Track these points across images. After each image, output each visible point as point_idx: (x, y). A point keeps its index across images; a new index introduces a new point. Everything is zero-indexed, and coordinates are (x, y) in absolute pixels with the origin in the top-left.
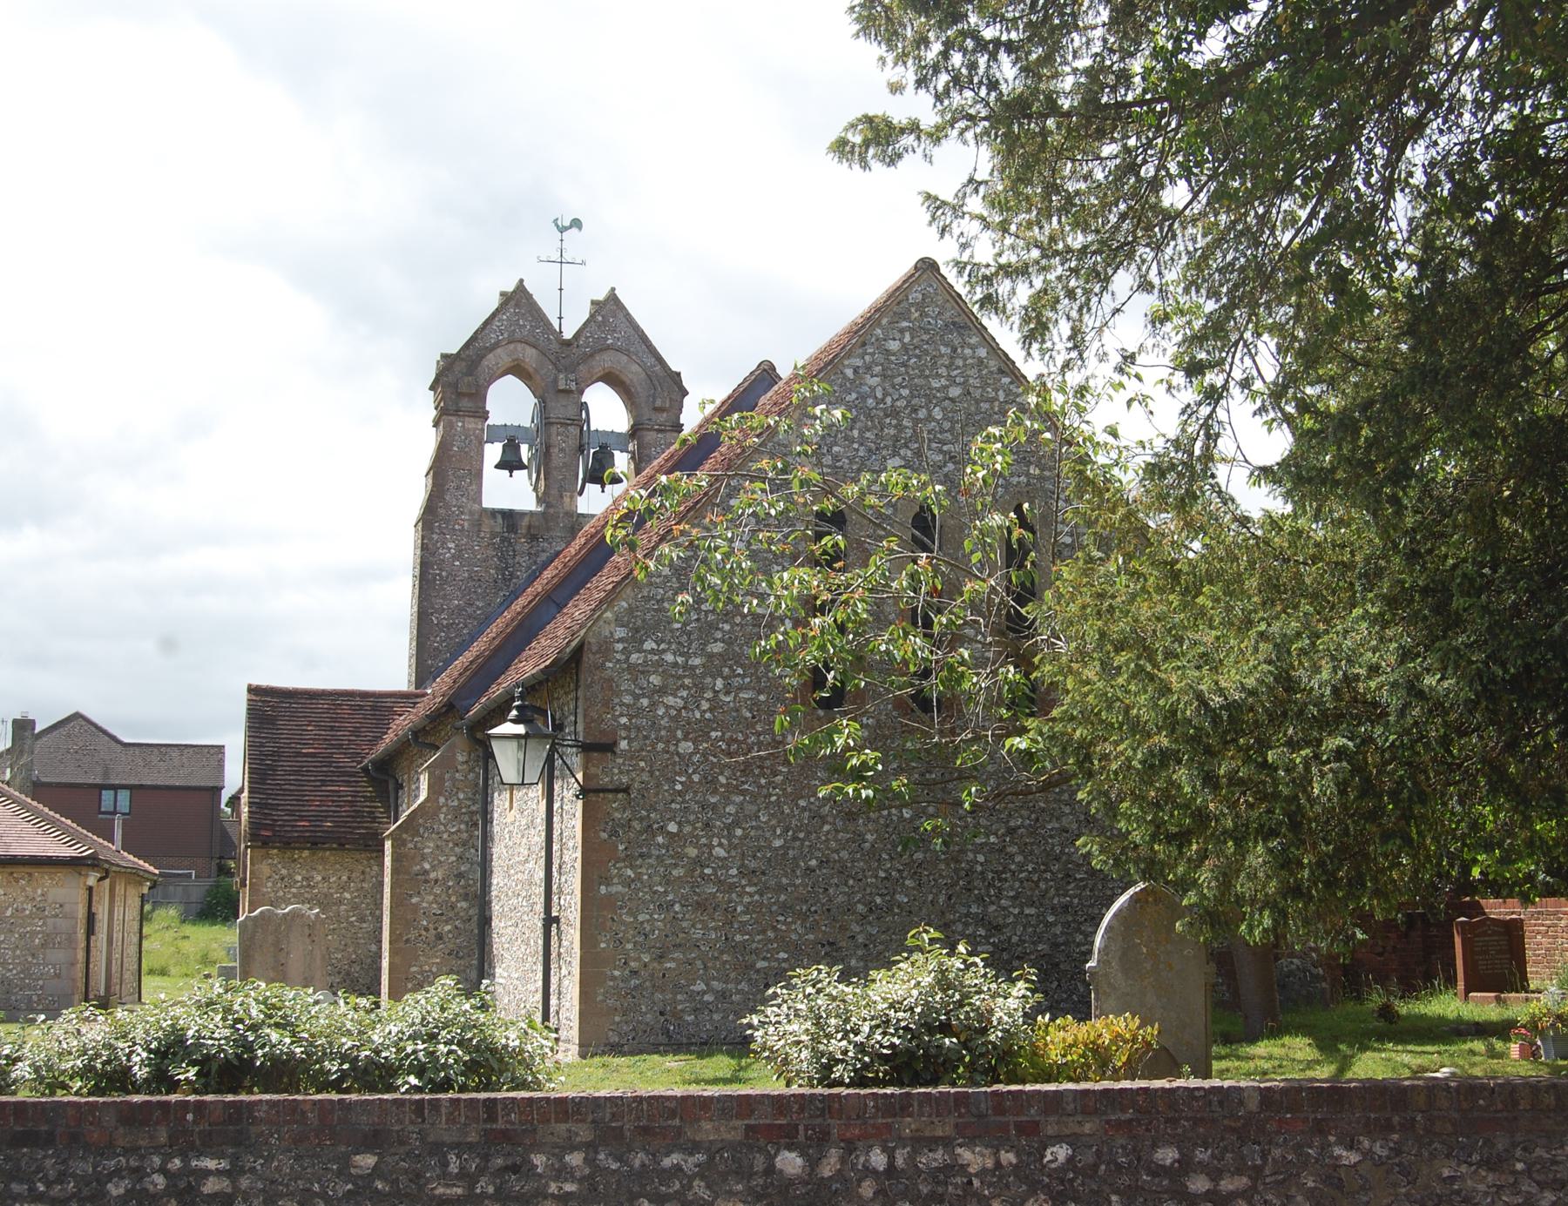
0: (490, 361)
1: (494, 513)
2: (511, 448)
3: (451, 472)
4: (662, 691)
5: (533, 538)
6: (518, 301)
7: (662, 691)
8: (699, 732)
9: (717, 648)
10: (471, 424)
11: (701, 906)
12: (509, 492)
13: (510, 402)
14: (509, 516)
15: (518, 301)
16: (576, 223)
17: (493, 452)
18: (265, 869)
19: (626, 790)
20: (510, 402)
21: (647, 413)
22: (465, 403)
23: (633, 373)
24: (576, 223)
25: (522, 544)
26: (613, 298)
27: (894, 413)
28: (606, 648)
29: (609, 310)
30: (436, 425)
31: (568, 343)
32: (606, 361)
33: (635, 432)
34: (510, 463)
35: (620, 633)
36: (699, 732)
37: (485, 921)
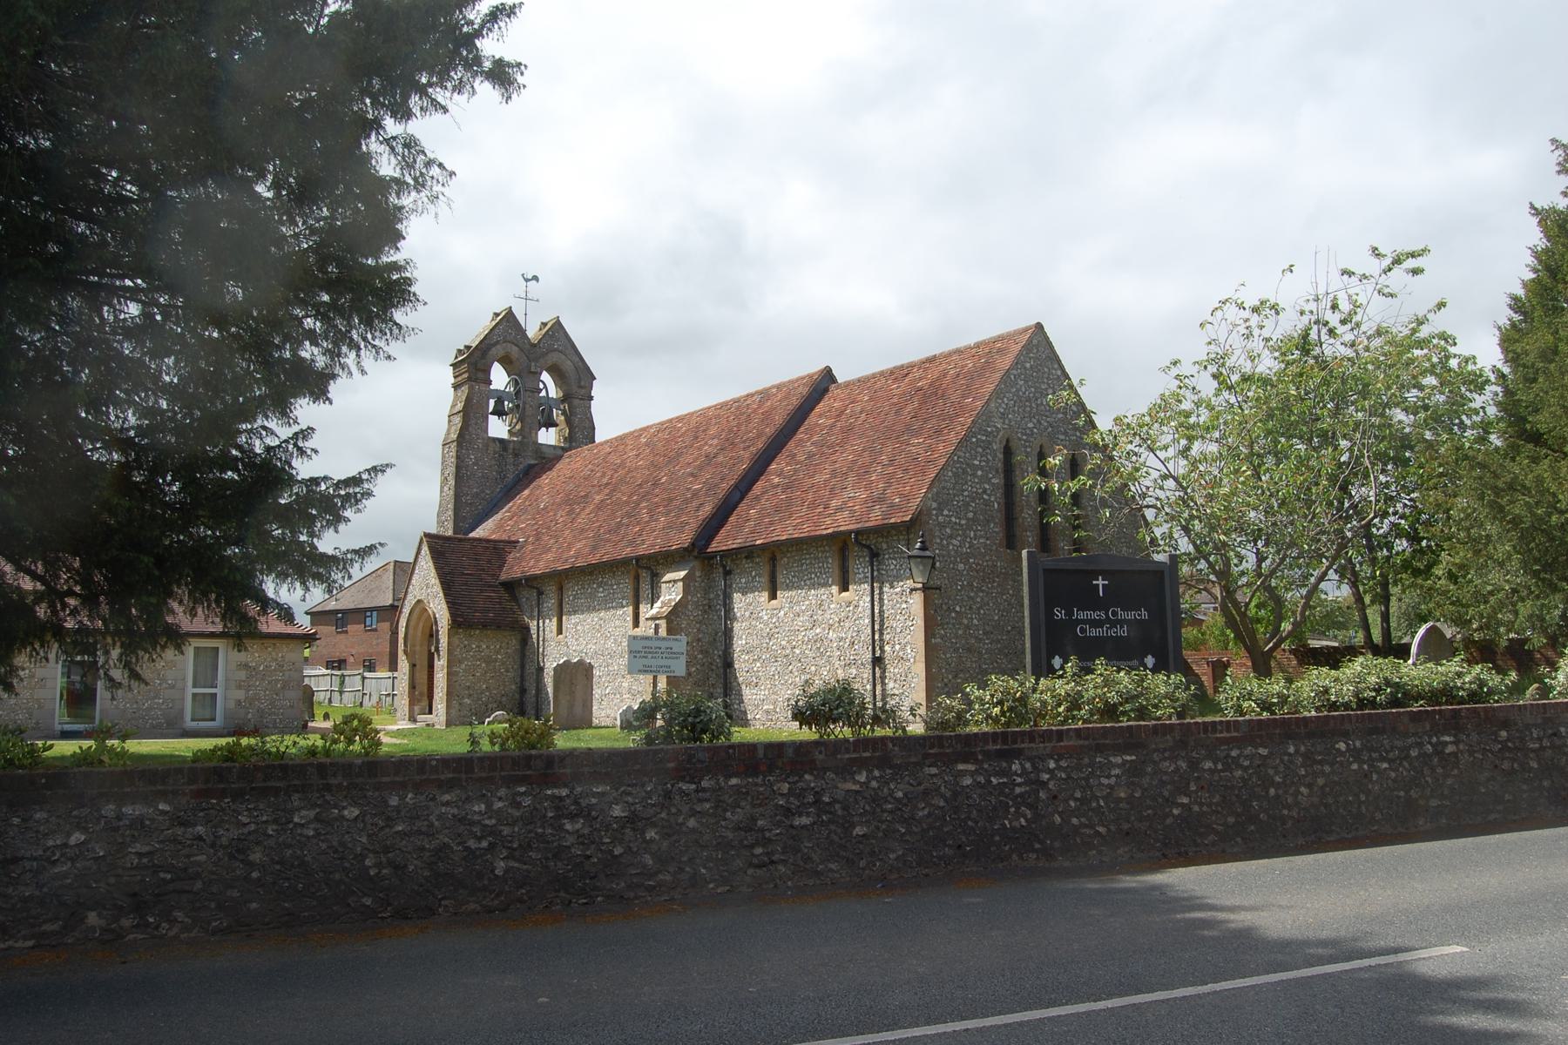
0: (494, 351)
1: (495, 440)
2: (499, 402)
3: (470, 416)
4: (951, 537)
5: (516, 455)
6: (508, 322)
7: (951, 537)
8: (965, 558)
9: (971, 515)
10: (483, 387)
11: (969, 650)
12: (498, 428)
13: (499, 378)
14: (501, 441)
15: (508, 322)
16: (535, 278)
17: (492, 403)
18: (456, 640)
19: (938, 588)
20: (499, 378)
21: (575, 388)
22: (480, 375)
23: (567, 366)
24: (535, 278)
25: (510, 459)
26: (558, 325)
27: (1029, 400)
28: (929, 514)
29: (556, 331)
30: (456, 387)
31: (534, 345)
32: (554, 358)
33: (567, 398)
34: (499, 412)
35: (934, 505)
36: (965, 558)
37: (728, 664)
